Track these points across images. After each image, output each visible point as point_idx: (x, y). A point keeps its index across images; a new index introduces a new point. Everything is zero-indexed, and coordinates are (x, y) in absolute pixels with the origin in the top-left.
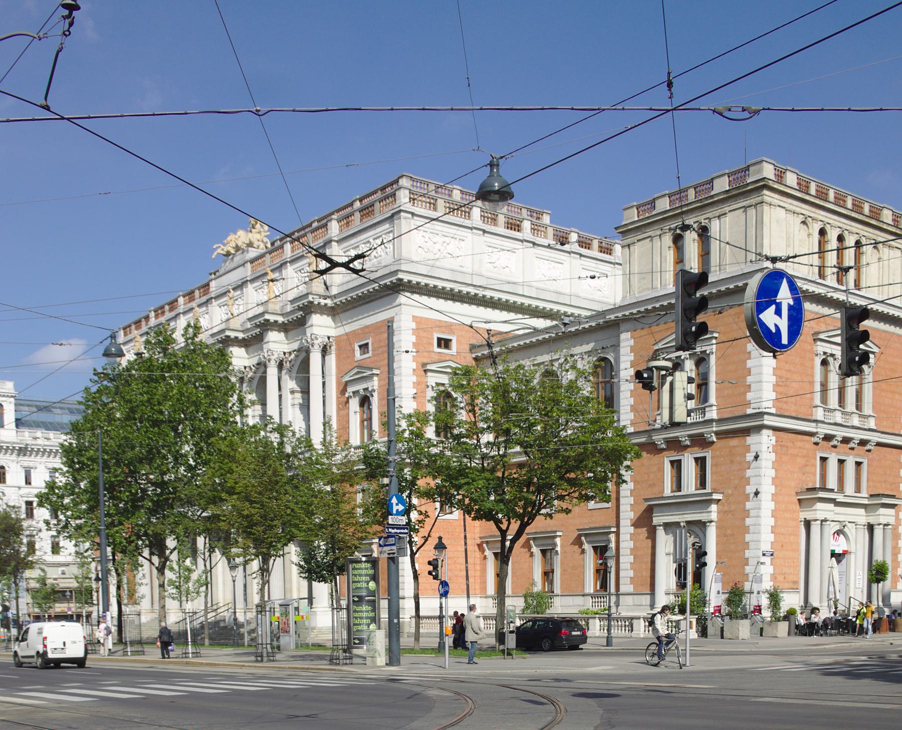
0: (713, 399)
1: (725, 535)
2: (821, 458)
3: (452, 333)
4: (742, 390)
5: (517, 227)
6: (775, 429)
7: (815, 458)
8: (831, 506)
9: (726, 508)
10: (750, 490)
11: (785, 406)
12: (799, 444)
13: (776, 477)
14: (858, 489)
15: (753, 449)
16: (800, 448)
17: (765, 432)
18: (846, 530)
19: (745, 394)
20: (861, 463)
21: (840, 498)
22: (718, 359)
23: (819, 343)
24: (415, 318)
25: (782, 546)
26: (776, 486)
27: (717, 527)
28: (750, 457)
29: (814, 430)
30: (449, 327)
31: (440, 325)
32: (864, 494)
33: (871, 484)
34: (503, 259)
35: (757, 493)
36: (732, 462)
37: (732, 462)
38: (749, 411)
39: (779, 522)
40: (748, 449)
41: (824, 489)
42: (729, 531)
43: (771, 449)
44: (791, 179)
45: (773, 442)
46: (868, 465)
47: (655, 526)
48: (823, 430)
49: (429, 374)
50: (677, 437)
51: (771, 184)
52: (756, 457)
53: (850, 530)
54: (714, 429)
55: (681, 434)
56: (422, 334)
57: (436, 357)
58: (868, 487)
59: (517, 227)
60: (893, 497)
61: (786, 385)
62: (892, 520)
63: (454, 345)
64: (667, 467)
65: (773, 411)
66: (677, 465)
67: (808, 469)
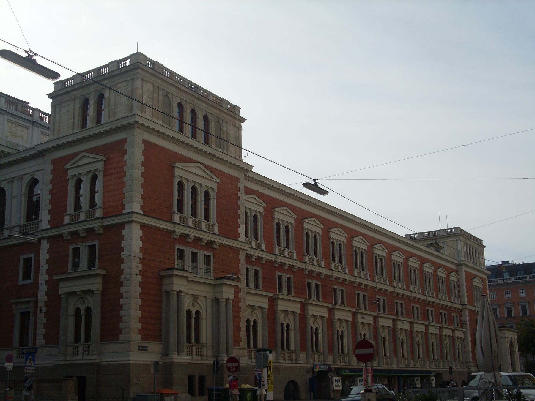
8: (184, 282)
32: (212, 278)
38: (124, 211)
47: (60, 295)
48: (179, 230)
50: (77, 231)
65: (142, 212)
66: (77, 251)
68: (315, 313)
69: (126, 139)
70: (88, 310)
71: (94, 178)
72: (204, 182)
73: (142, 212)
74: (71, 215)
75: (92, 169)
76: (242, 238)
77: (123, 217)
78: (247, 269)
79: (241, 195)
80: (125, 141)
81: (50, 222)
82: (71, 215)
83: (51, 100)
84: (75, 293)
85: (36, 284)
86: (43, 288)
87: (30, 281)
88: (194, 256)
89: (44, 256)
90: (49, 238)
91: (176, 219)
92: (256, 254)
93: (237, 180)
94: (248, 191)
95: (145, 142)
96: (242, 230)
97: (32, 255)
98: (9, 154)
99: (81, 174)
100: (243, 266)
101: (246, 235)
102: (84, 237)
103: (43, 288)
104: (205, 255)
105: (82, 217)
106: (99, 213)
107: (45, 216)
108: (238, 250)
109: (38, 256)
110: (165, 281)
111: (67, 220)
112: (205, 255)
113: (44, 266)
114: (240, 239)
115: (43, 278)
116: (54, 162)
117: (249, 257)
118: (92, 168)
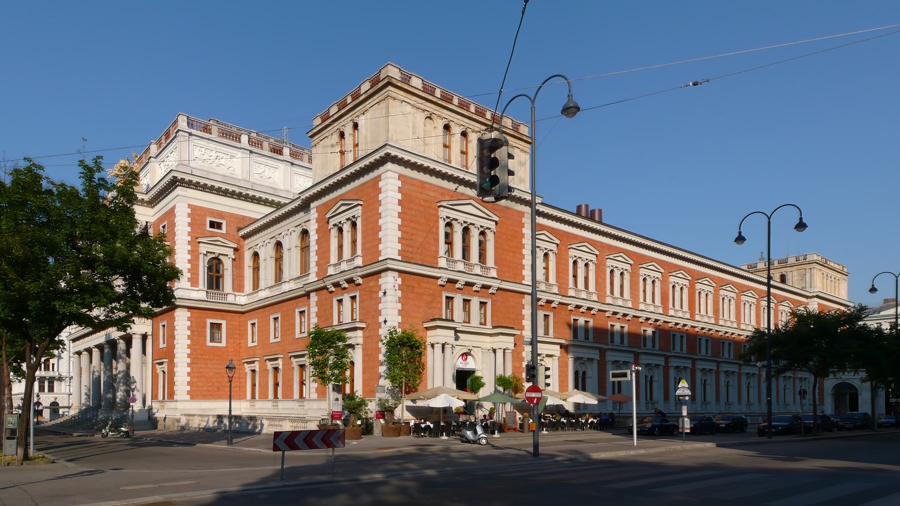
0: (359, 251)
1: (368, 355)
2: (447, 297)
5: (280, 152)
7: (441, 297)
9: (368, 334)
10: (381, 319)
11: (411, 255)
12: (425, 285)
15: (383, 288)
16: (426, 288)
17: (390, 273)
20: (485, 303)
22: (362, 221)
23: (442, 209)
24: (190, 206)
27: (363, 350)
28: (381, 294)
29: (439, 275)
31: (212, 212)
34: (268, 172)
36: (371, 298)
37: (371, 298)
38: (380, 259)
41: (452, 321)
42: (370, 352)
43: (397, 287)
44: (416, 82)
49: (201, 245)
51: (394, 81)
52: (385, 293)
54: (360, 274)
55: (341, 279)
56: (196, 217)
57: (209, 234)
58: (492, 321)
59: (280, 152)
60: (513, 328)
61: (411, 239)
63: (224, 226)
64: (335, 304)
65: (400, 258)
67: (433, 305)
72: (479, 222)
73: (400, 258)
74: (335, 265)
81: (317, 274)
89: (314, 309)
90: (316, 290)
91: (442, 263)
93: (522, 214)
96: (527, 272)
97: (305, 309)
98: (285, 205)
106: (359, 262)
107: (313, 268)
109: (309, 310)
111: (331, 271)
114: (524, 282)
118: (349, 214)
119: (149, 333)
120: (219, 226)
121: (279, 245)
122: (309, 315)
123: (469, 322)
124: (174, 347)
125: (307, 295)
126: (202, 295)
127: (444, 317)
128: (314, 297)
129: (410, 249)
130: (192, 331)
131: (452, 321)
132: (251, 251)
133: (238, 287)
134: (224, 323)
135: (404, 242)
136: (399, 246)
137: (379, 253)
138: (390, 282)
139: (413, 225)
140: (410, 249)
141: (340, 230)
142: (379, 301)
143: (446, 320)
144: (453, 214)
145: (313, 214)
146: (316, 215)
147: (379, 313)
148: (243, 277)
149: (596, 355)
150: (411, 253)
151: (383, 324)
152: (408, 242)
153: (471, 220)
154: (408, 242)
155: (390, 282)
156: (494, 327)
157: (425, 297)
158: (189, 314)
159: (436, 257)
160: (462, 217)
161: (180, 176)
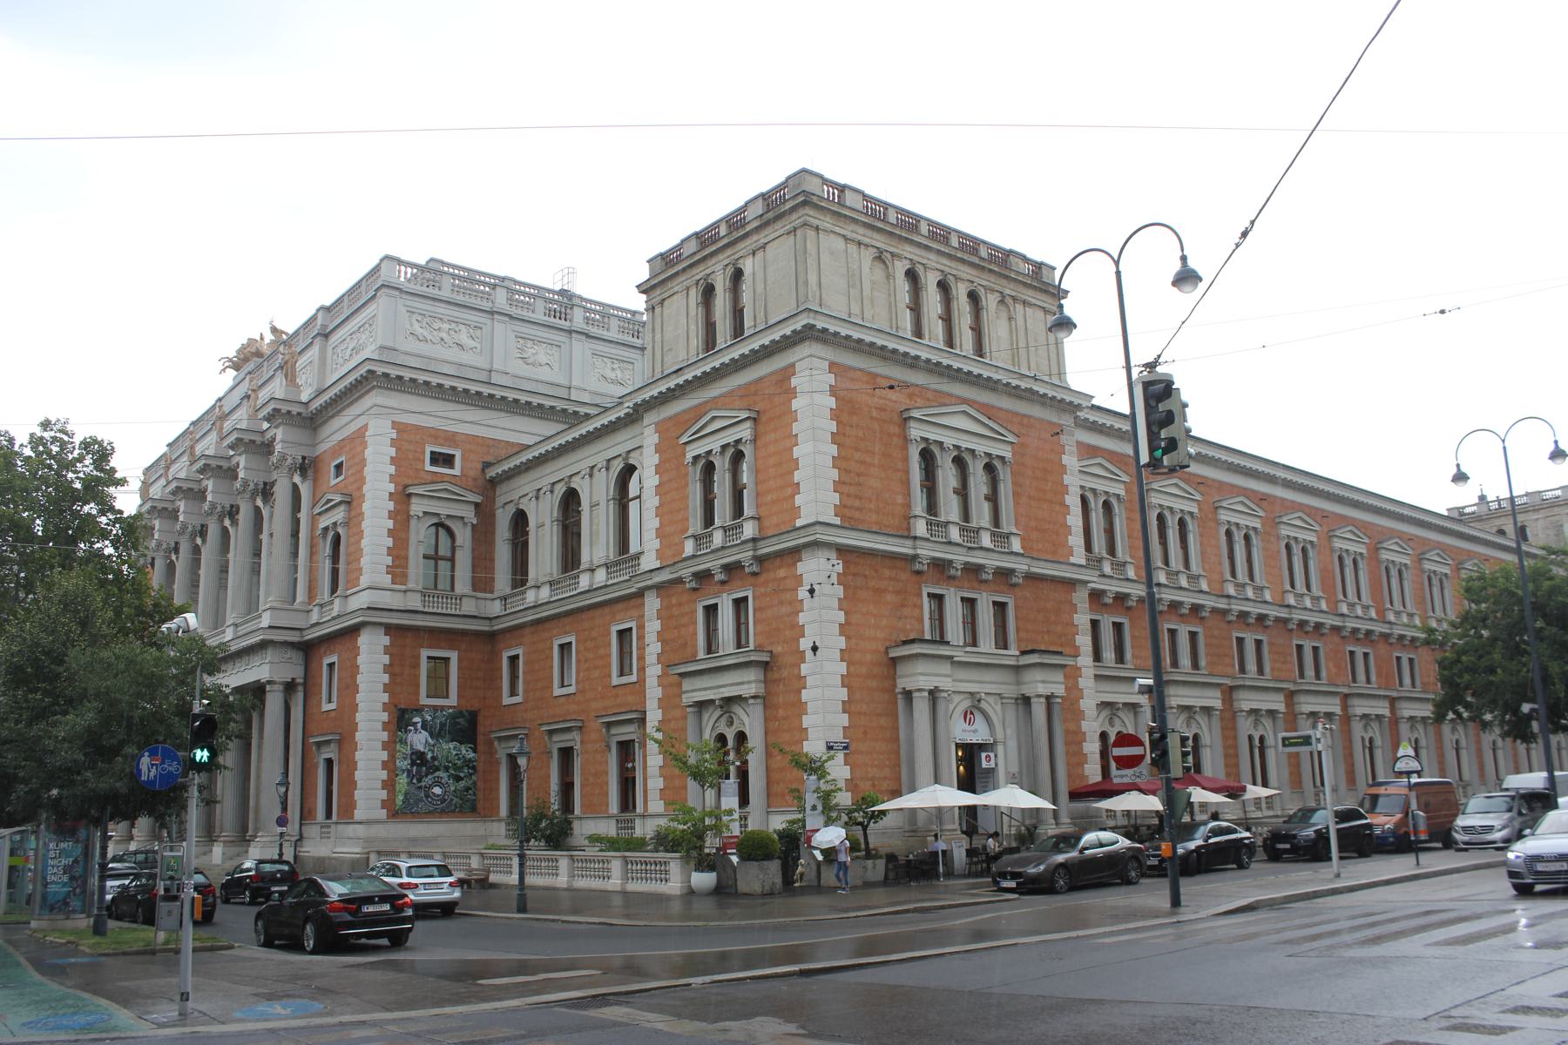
3: (456, 446)
4: (789, 491)
6: (843, 551)
7: (920, 595)
8: (946, 668)
10: (805, 644)
11: (857, 515)
13: (847, 623)
14: (1002, 642)
18: (983, 705)
19: (793, 496)
21: (960, 656)
25: (865, 733)
26: (848, 638)
28: (803, 593)
29: (910, 552)
30: (451, 439)
33: (1023, 635)
35: (815, 649)
38: (799, 523)
39: (858, 695)
40: (799, 580)
41: (943, 642)
43: (834, 579)
45: (840, 568)
46: (1016, 607)
50: (709, 570)
52: (812, 591)
53: (992, 707)
58: (1019, 640)
60: (1060, 653)
62: (1059, 690)
65: (837, 521)
66: (711, 611)
67: (906, 611)
68: (1255, 706)
69: (793, 365)
70: (741, 737)
71: (738, 457)
73: (837, 521)
74: (696, 538)
75: (731, 440)
76: (1079, 557)
77: (795, 535)
78: (1095, 624)
79: (1070, 460)
80: (789, 371)
82: (696, 538)
83: (644, 297)
84: (712, 702)
85: (641, 681)
86: (654, 692)
87: (634, 678)
88: (970, 603)
89: (653, 626)
90: (659, 587)
91: (920, 528)
92: (1113, 587)
94: (1089, 451)
95: (834, 367)
96: (1076, 540)
97: (633, 624)
99: (738, 441)
100: (1082, 619)
101: (1088, 547)
102: (723, 583)
103: (654, 692)
104: (995, 603)
105: (718, 538)
108: (1071, 584)
109: (641, 627)
110: (902, 669)
112: (995, 603)
113: (654, 648)
114: (1072, 560)
115: (653, 671)
116: (661, 428)
117: (1096, 596)
118: (729, 437)
119: (300, 681)
120: (448, 460)
121: (571, 499)
122: (641, 638)
123: (974, 644)
124: (354, 708)
125: (640, 594)
126: (415, 602)
127: (928, 637)
128: (652, 603)
129: (857, 503)
130: (393, 675)
131: (943, 642)
132: (511, 510)
133: (482, 583)
134: (453, 656)
135: (846, 489)
136: (836, 498)
137: (796, 512)
138: (817, 569)
139: (857, 455)
140: (857, 503)
141: (709, 469)
142: (797, 607)
143: (932, 642)
144: (933, 435)
145: (648, 436)
146: (655, 438)
147: (800, 631)
148: (492, 560)
149: (1214, 700)
150: (858, 509)
151: (809, 654)
152: (852, 490)
153: (966, 443)
154: (852, 490)
155: (817, 569)
156: (1023, 653)
157: (889, 597)
158: (386, 640)
159: (908, 518)
160: (949, 440)
161: (380, 369)
